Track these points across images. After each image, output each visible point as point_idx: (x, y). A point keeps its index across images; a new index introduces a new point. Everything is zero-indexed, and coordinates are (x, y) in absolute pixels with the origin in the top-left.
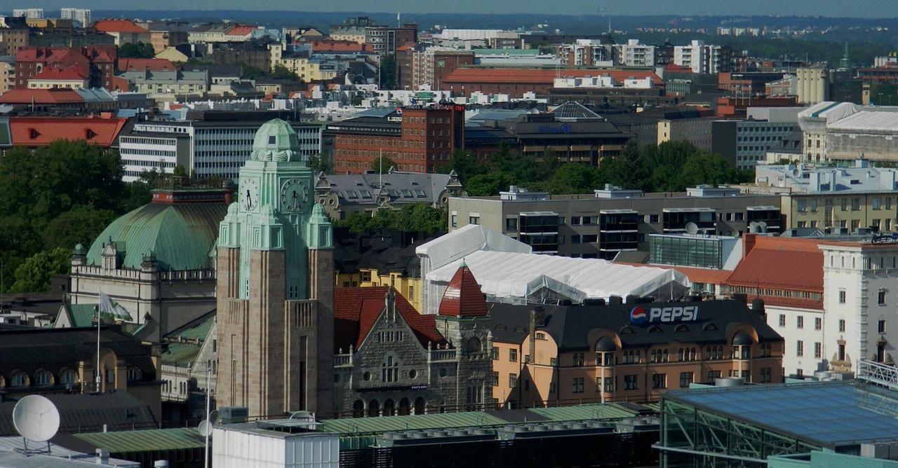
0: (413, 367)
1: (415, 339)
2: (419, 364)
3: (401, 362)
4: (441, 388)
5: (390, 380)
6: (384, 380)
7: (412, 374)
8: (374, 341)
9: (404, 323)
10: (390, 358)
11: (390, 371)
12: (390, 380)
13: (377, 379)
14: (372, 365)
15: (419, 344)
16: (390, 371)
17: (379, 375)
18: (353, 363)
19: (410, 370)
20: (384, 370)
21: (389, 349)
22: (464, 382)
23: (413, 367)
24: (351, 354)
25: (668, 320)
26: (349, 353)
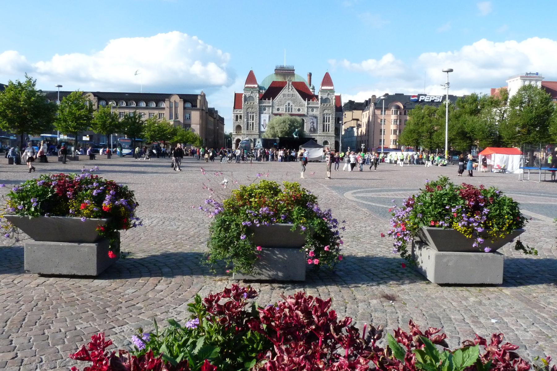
0: (299, 107)
1: (300, 97)
3: (293, 105)
5: (289, 111)
6: (286, 111)
7: (299, 110)
9: (295, 90)
10: (289, 104)
11: (289, 108)
12: (289, 111)
15: (302, 99)
16: (289, 108)
20: (286, 108)
21: (288, 100)
23: (299, 107)
24: (271, 101)
25: (428, 101)
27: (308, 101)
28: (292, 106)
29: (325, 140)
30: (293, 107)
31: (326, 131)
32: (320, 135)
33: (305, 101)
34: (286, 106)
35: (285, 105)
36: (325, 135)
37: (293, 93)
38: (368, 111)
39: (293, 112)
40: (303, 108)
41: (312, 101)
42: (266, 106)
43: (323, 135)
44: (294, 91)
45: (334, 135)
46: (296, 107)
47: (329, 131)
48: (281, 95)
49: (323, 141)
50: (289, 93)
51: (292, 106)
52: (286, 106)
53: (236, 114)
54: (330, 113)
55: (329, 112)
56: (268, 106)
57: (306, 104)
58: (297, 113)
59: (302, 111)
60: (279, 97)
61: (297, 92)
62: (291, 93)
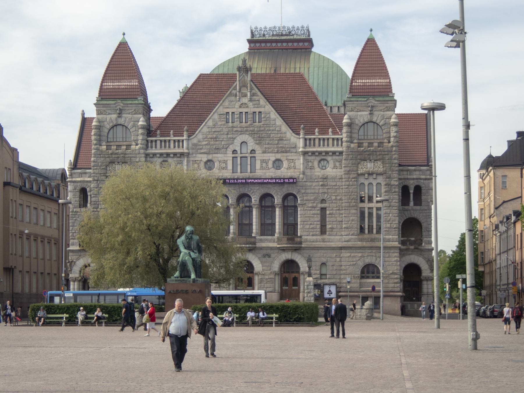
0: (279, 156)
1: (279, 121)
2: (286, 152)
3: (258, 148)
4: (321, 183)
7: (278, 164)
8: (220, 123)
9: (263, 101)
13: (223, 168)
14: (216, 151)
15: (285, 128)
17: (226, 164)
18: (188, 149)
19: (273, 159)
21: (242, 133)
22: (351, 176)
23: (279, 156)
26: (183, 136)
27: (305, 134)
28: (253, 151)
29: (368, 261)
30: (259, 156)
31: (370, 231)
32: (350, 244)
33: (299, 134)
34: (234, 152)
35: (231, 148)
36: (365, 244)
37: (257, 110)
39: (259, 173)
40: (291, 156)
41: (320, 133)
42: (168, 155)
43: (359, 244)
44: (258, 105)
45: (396, 244)
46: (266, 156)
47: (379, 231)
48: (216, 116)
49: (361, 264)
50: (244, 110)
51: (253, 151)
52: (234, 152)
53: (79, 186)
54: (381, 170)
55: (379, 167)
56: (175, 154)
57: (301, 143)
58: (271, 173)
59: (289, 168)
60: (210, 123)
61: (269, 108)
62: (251, 109)
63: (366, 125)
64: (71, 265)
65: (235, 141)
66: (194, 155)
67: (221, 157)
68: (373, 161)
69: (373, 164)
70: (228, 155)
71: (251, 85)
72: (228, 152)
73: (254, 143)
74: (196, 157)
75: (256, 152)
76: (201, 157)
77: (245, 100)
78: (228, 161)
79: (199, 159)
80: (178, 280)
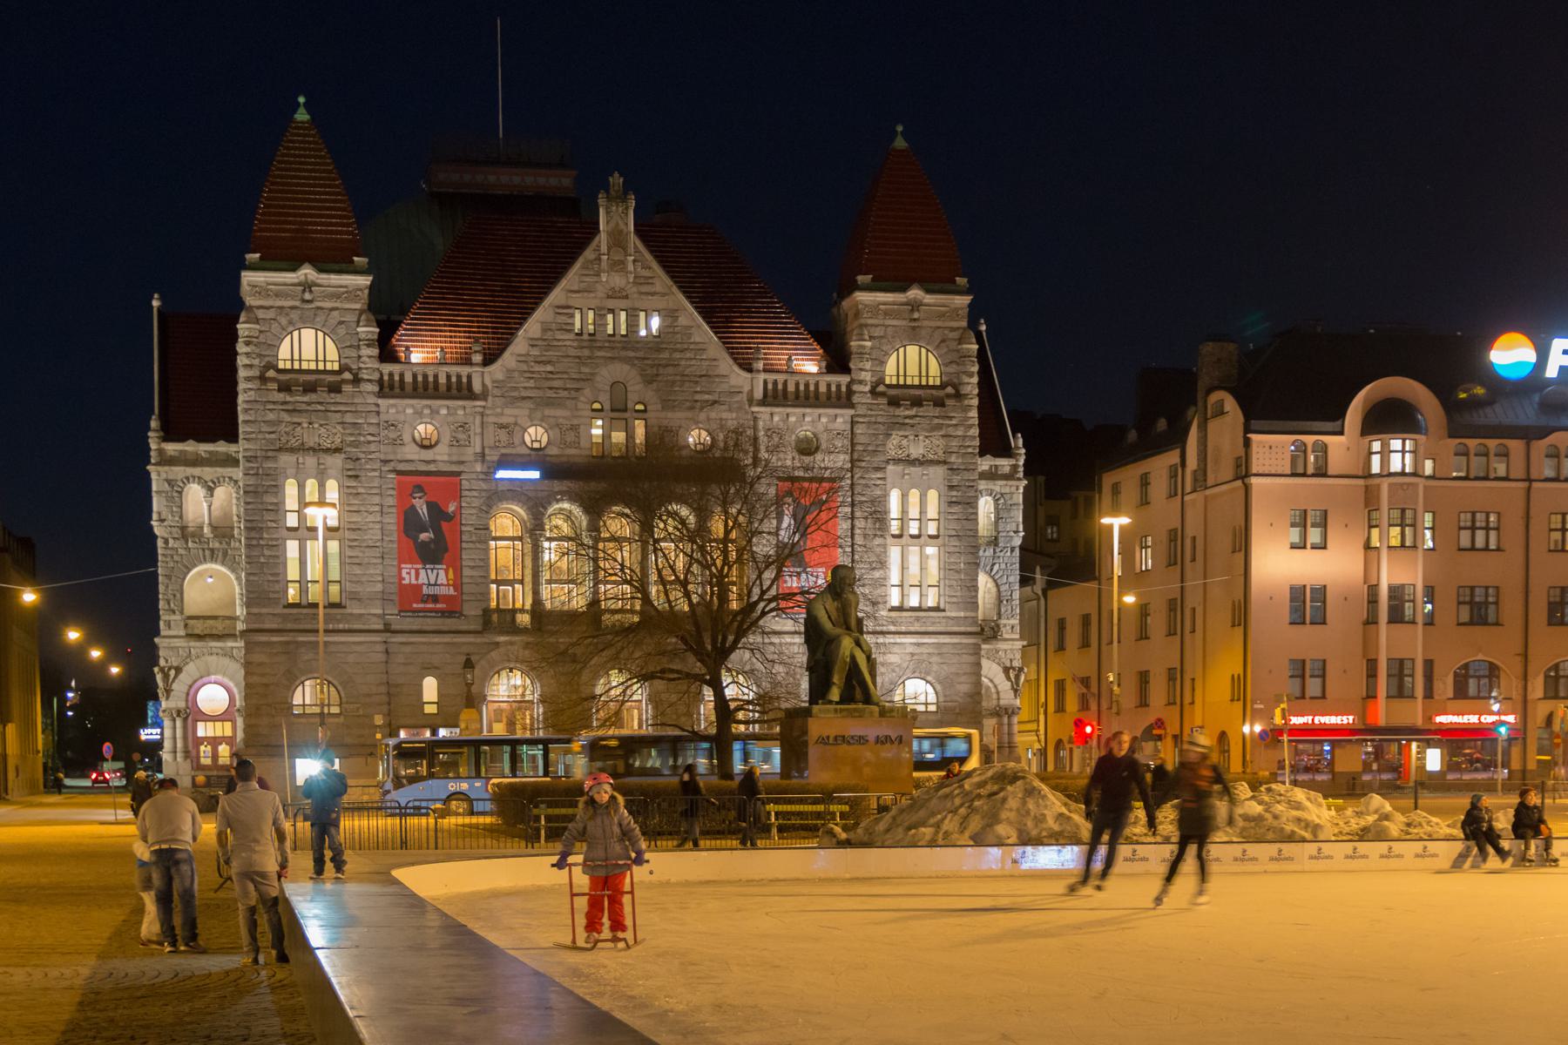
38: (1173, 457)
63: (902, 350)
64: (166, 676)
65: (598, 378)
66: (499, 410)
67: (564, 418)
68: (921, 438)
69: (922, 444)
70: (580, 413)
71: (636, 247)
72: (580, 405)
73: (641, 385)
74: (502, 414)
75: (648, 408)
76: (516, 416)
77: (618, 281)
78: (582, 427)
79: (511, 420)
80: (841, 710)
